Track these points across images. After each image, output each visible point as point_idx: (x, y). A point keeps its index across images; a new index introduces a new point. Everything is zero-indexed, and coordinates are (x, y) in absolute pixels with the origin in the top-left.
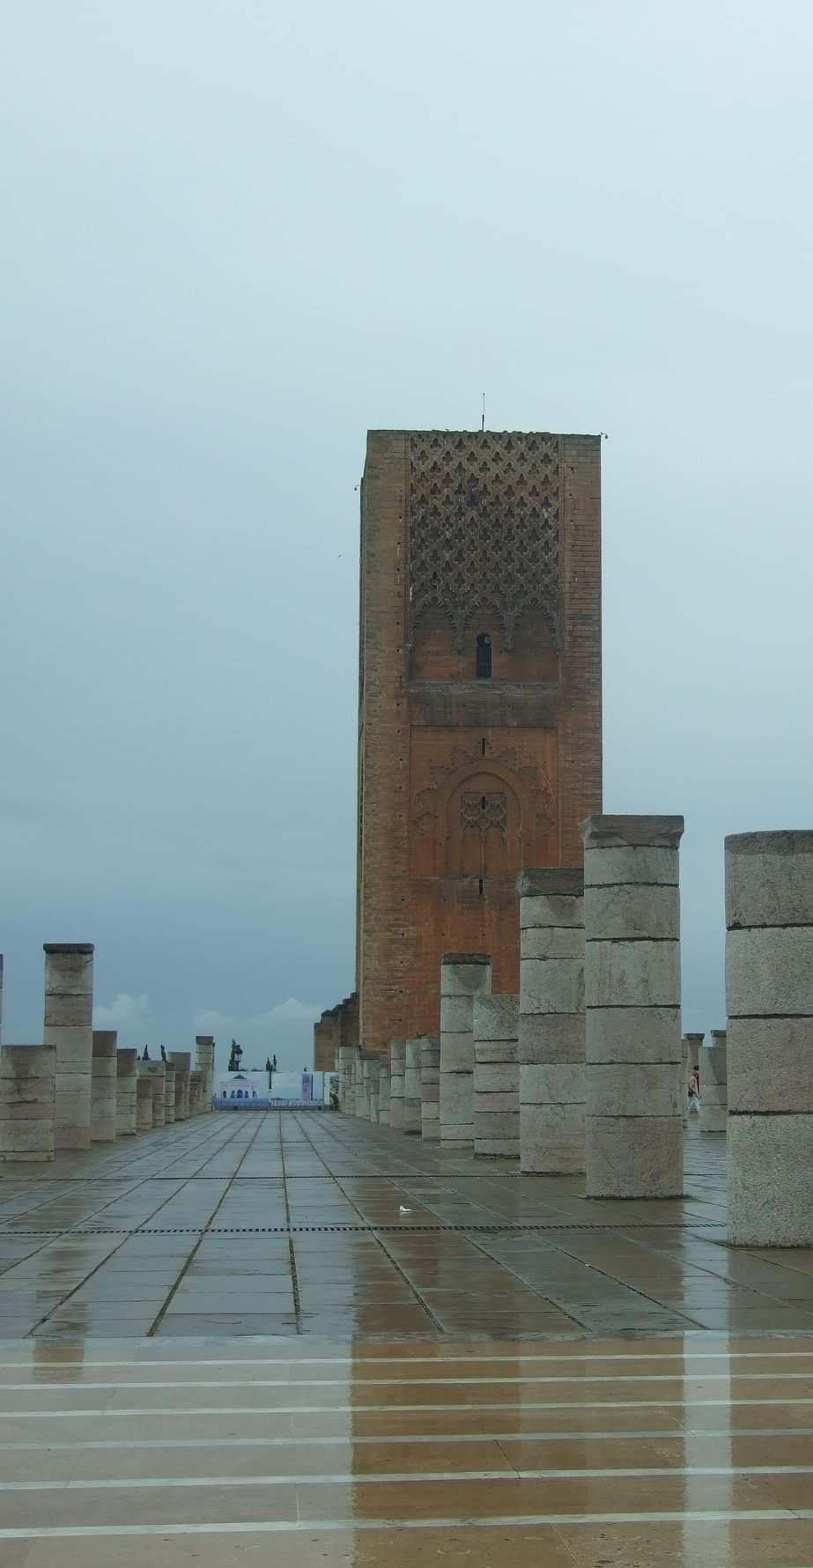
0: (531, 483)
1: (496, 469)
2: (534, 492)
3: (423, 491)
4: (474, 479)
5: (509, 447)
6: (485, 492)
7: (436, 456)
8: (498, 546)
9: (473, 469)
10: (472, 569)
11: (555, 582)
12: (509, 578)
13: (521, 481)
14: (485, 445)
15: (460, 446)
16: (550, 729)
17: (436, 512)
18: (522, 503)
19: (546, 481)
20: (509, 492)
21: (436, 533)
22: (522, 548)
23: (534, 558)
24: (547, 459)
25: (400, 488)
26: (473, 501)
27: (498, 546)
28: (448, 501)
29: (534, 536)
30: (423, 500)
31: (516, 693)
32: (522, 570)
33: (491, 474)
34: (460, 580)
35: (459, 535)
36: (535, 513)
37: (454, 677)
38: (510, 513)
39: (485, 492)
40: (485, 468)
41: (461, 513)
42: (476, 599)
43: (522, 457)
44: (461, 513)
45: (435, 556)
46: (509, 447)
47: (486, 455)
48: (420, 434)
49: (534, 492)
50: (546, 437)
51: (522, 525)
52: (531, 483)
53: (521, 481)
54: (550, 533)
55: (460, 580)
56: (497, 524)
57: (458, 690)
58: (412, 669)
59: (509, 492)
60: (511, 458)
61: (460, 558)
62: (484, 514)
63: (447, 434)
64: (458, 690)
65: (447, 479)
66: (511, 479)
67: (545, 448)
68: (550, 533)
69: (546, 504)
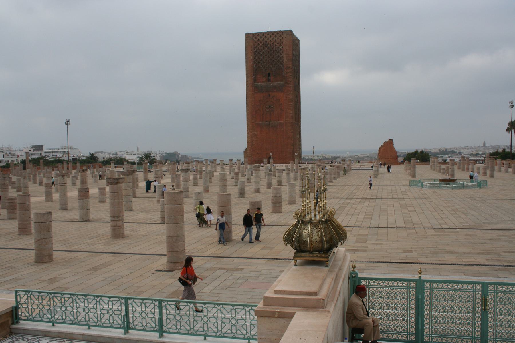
0: (277, 41)
1: (270, 39)
2: (278, 43)
3: (256, 45)
4: (266, 41)
5: (273, 34)
6: (268, 44)
7: (258, 38)
8: (271, 55)
9: (266, 39)
10: (266, 60)
11: (283, 61)
12: (273, 61)
13: (275, 41)
14: (268, 34)
15: (263, 35)
16: (282, 91)
17: (259, 49)
18: (276, 46)
19: (280, 40)
20: (273, 43)
21: (259, 53)
22: (276, 55)
23: (278, 57)
24: (280, 36)
25: (251, 45)
26: (266, 46)
27: (271, 55)
28: (261, 47)
29: (278, 52)
30: (256, 47)
31: (275, 84)
32: (276, 59)
33: (269, 40)
34: (264, 62)
35: (263, 53)
36: (278, 47)
37: (263, 82)
38: (273, 48)
39: (268, 44)
40: (268, 39)
41: (264, 49)
42: (267, 66)
43: (275, 36)
44: (264, 49)
45: (259, 58)
46: (273, 34)
47: (269, 36)
48: (255, 33)
49: (278, 43)
50: (280, 31)
51: (276, 50)
52: (277, 41)
53: (275, 41)
54: (281, 51)
55: (264, 62)
56: (271, 50)
57: (264, 84)
58: (255, 81)
59: (273, 43)
60: (273, 36)
61: (264, 58)
62: (268, 48)
63: (260, 33)
64: (264, 84)
65: (261, 42)
66: (273, 41)
67: (280, 34)
68: (281, 51)
69: (280, 45)
